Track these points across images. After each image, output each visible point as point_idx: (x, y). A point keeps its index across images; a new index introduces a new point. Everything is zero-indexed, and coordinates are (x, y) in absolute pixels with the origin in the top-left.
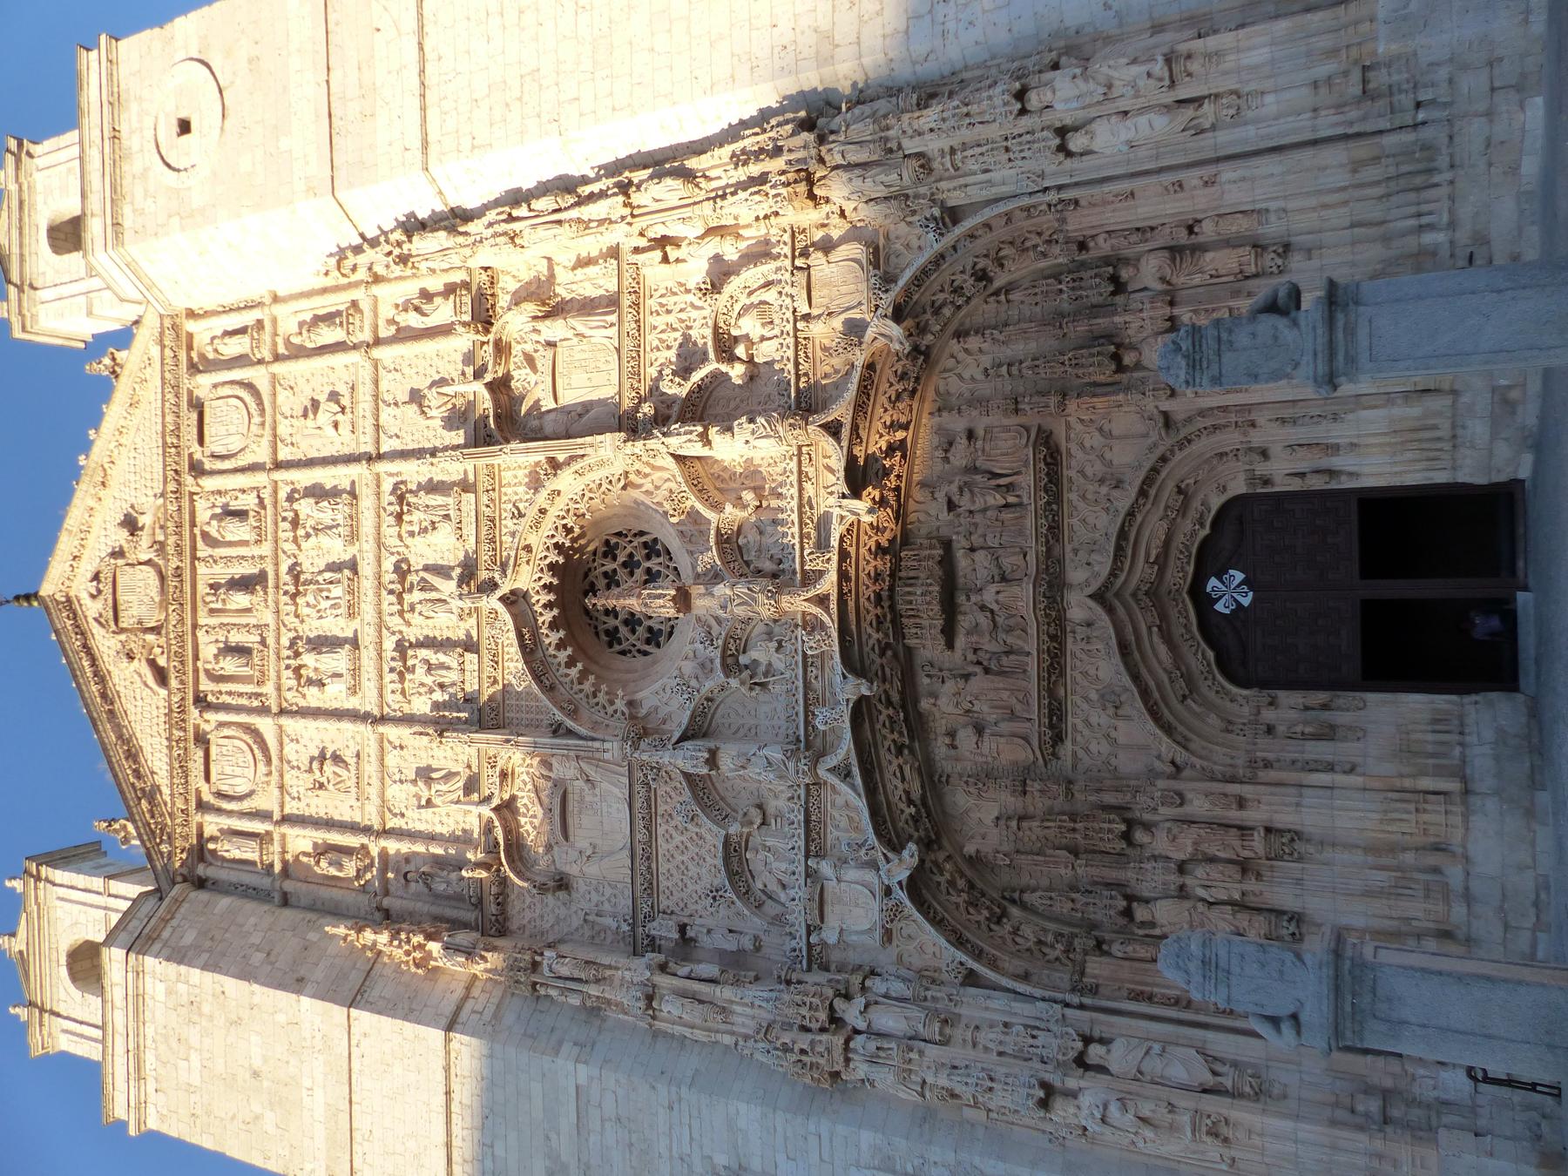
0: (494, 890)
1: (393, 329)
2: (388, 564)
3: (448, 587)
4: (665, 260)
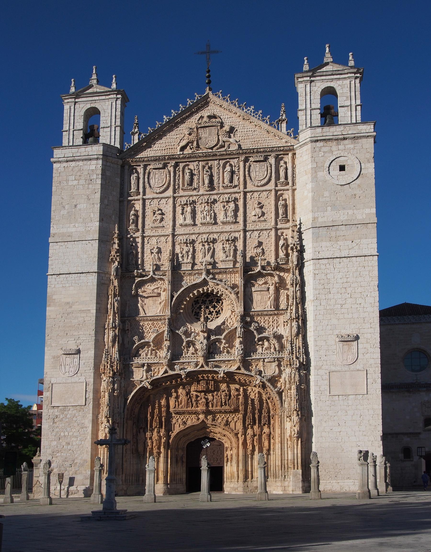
0: (132, 276)
1: (280, 234)
2: (216, 236)
3: (208, 258)
4: (284, 322)
